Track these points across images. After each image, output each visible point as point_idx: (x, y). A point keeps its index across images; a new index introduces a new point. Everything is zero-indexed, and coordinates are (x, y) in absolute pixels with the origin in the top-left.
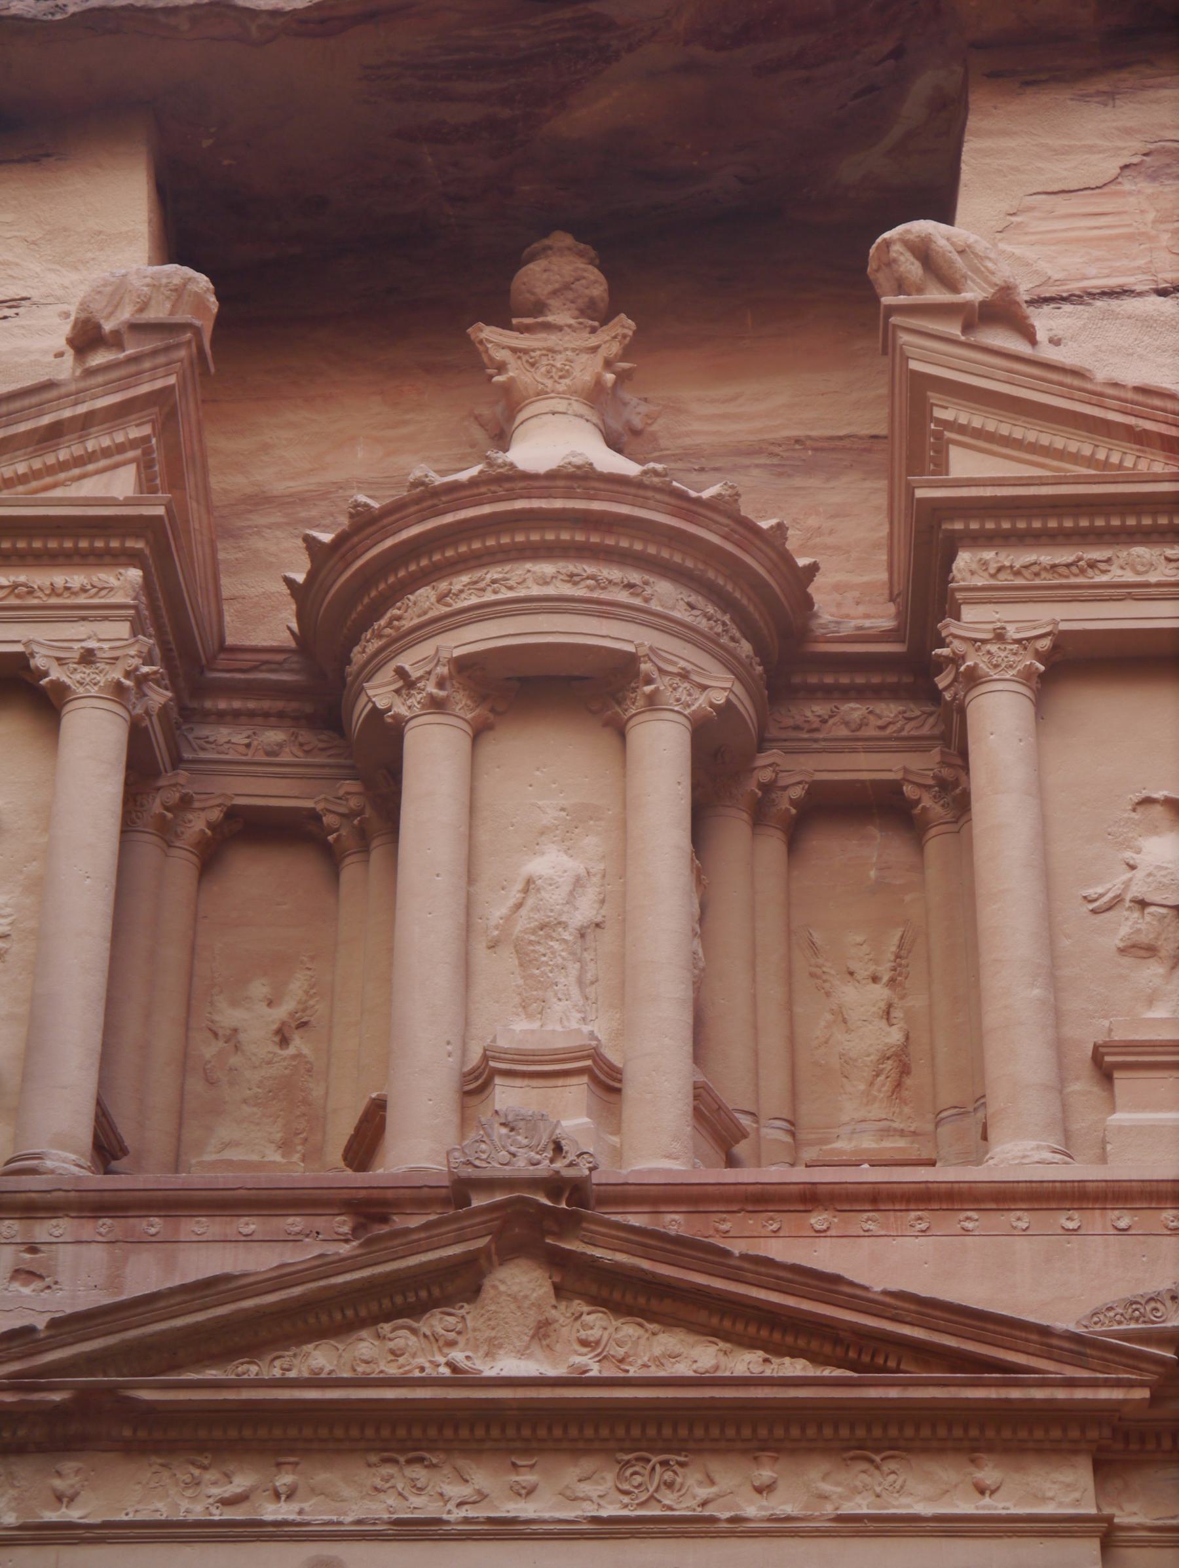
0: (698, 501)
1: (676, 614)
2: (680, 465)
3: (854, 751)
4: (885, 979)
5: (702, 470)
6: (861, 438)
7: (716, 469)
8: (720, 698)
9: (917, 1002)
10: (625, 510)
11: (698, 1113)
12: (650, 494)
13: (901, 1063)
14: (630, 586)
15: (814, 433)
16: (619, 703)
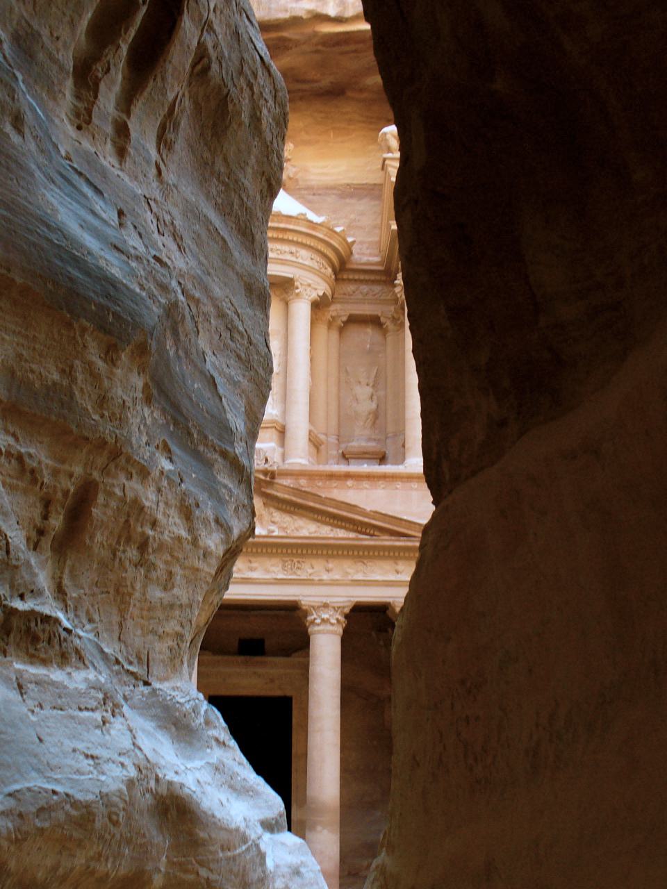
0: (316, 224)
1: (306, 263)
2: (306, 192)
3: (364, 303)
4: (371, 384)
5: (314, 194)
6: (370, 185)
7: (320, 195)
8: (321, 294)
9: (381, 393)
10: (291, 227)
11: (310, 439)
12: (300, 221)
13: (376, 415)
14: (291, 253)
15: (355, 182)
16: (287, 293)
